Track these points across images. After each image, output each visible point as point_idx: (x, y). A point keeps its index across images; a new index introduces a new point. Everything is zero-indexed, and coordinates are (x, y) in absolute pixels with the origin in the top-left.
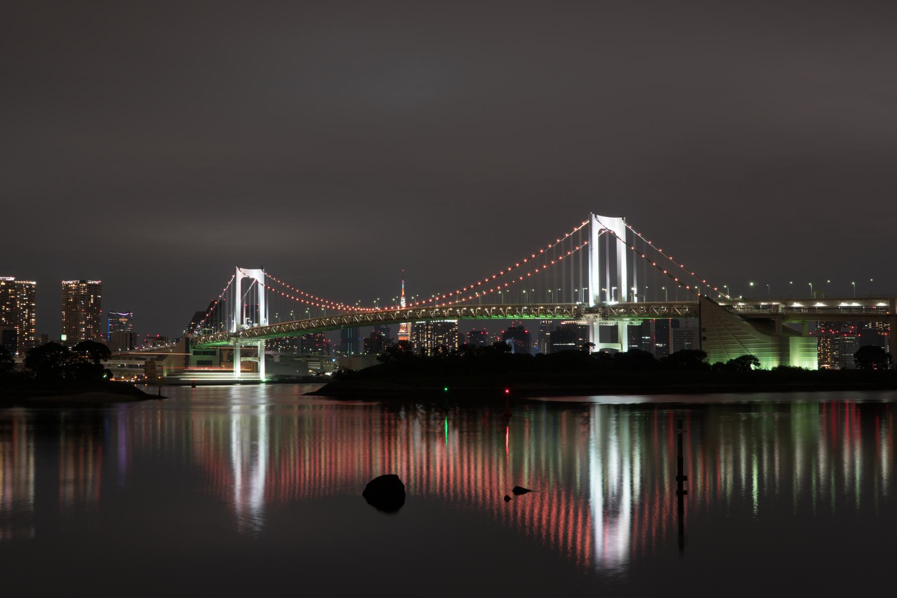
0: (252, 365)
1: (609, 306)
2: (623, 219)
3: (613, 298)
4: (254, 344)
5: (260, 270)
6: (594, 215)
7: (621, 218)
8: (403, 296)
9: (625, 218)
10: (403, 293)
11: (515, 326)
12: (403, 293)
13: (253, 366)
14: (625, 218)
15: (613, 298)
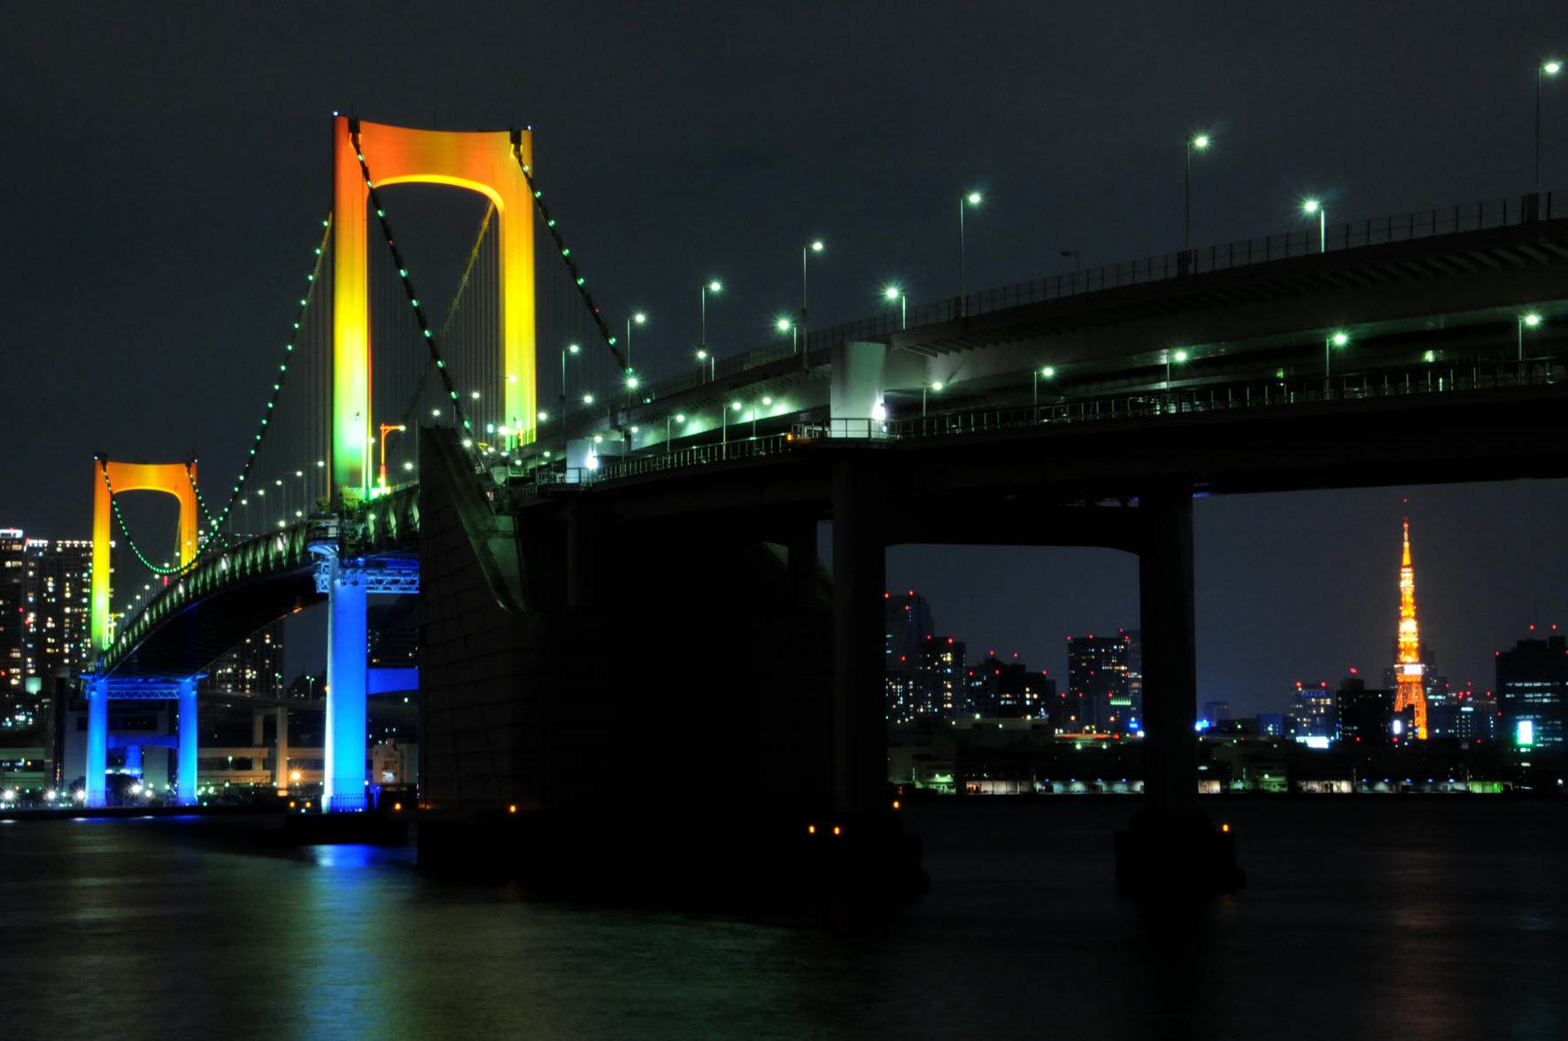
0: (397, 754)
1: (366, 507)
2: (516, 140)
3: (383, 469)
4: (163, 692)
5: (183, 467)
6: (343, 125)
7: (507, 135)
8: (1408, 566)
9: (526, 136)
10: (1406, 559)
11: (1537, 638)
12: (1406, 559)
13: (402, 756)
14: (526, 136)
15: (383, 469)
